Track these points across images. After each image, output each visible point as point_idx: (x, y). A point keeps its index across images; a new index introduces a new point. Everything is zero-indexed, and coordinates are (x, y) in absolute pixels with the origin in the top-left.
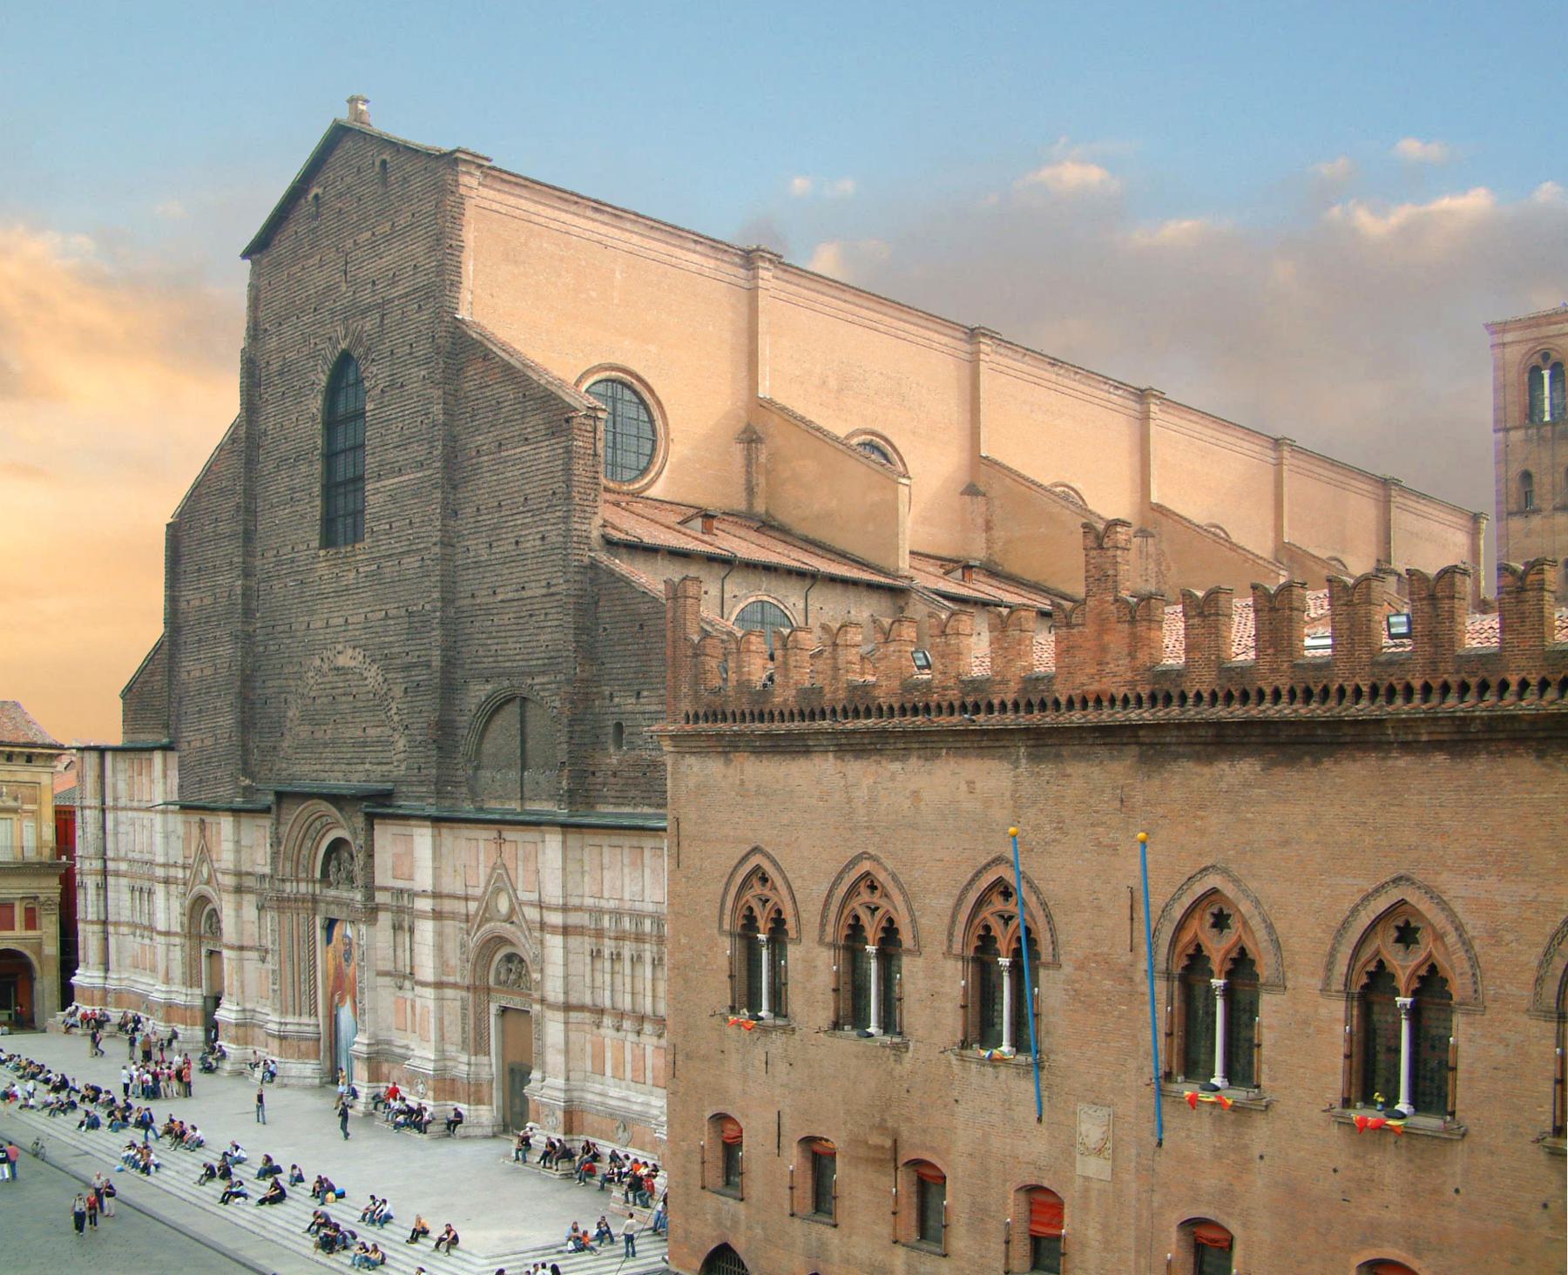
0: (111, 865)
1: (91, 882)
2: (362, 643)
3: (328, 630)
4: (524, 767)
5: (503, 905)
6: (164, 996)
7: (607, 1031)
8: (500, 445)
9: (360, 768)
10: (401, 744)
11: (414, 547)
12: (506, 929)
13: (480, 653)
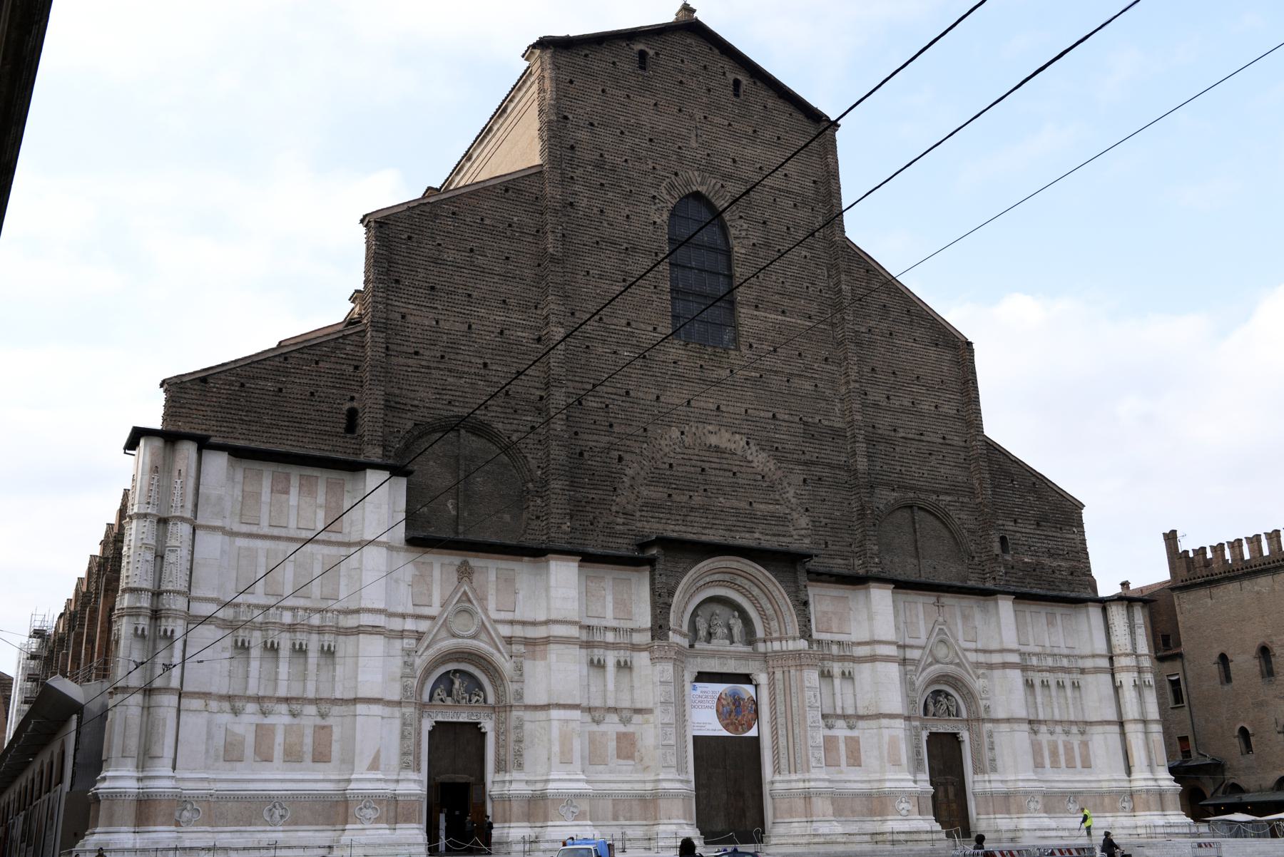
1: (178, 628)
2: (743, 431)
3: (692, 410)
7: (1044, 737)
8: (891, 334)
9: (747, 535)
10: (804, 521)
11: (806, 374)
12: (951, 669)
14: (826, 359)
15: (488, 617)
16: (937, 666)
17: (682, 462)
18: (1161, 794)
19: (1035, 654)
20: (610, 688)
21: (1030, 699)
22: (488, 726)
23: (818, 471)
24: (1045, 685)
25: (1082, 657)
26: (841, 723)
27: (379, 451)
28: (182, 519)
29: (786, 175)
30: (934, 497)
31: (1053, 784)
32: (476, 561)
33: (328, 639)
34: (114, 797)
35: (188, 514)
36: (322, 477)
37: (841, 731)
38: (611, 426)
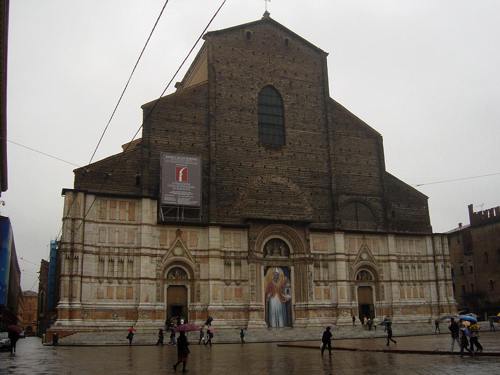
1: (80, 255)
9: (287, 215)
10: (310, 209)
13: (344, 187)
14: (321, 146)
15: (187, 249)
16: (362, 262)
18: (450, 306)
19: (403, 256)
21: (400, 273)
24: (407, 267)
25: (423, 256)
28: (79, 219)
29: (306, 75)
30: (365, 197)
32: (183, 229)
33: (131, 258)
34: (62, 309)
35: (82, 217)
37: (322, 287)
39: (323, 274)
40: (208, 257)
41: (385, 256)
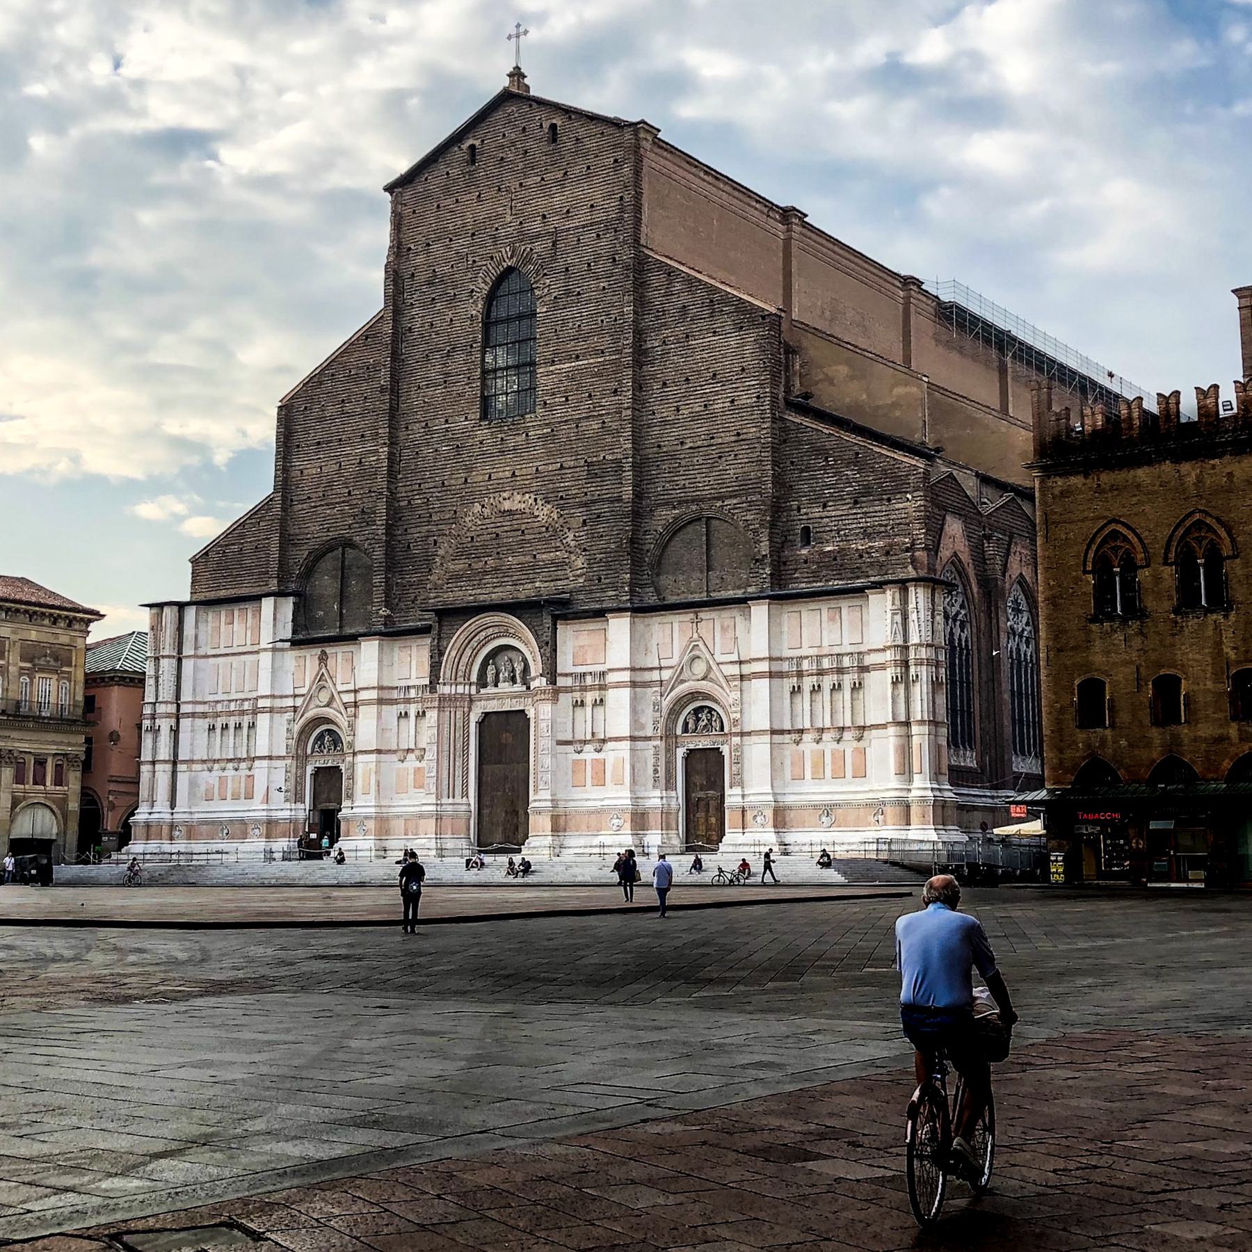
0: (185, 709)
1: (165, 725)
4: (709, 568)
5: (699, 668)
6: (265, 813)
8: (687, 337)
9: (530, 586)
10: (579, 562)
12: (704, 686)
14: (616, 391)
17: (480, 532)
20: (407, 734)
22: (343, 767)
23: (596, 509)
26: (588, 747)
27: (275, 581)
28: (163, 657)
30: (719, 504)
31: (803, 797)
32: (329, 650)
36: (250, 607)
37: (589, 754)
38: (431, 516)
39: (584, 724)
40: (356, 705)
41: (749, 662)
